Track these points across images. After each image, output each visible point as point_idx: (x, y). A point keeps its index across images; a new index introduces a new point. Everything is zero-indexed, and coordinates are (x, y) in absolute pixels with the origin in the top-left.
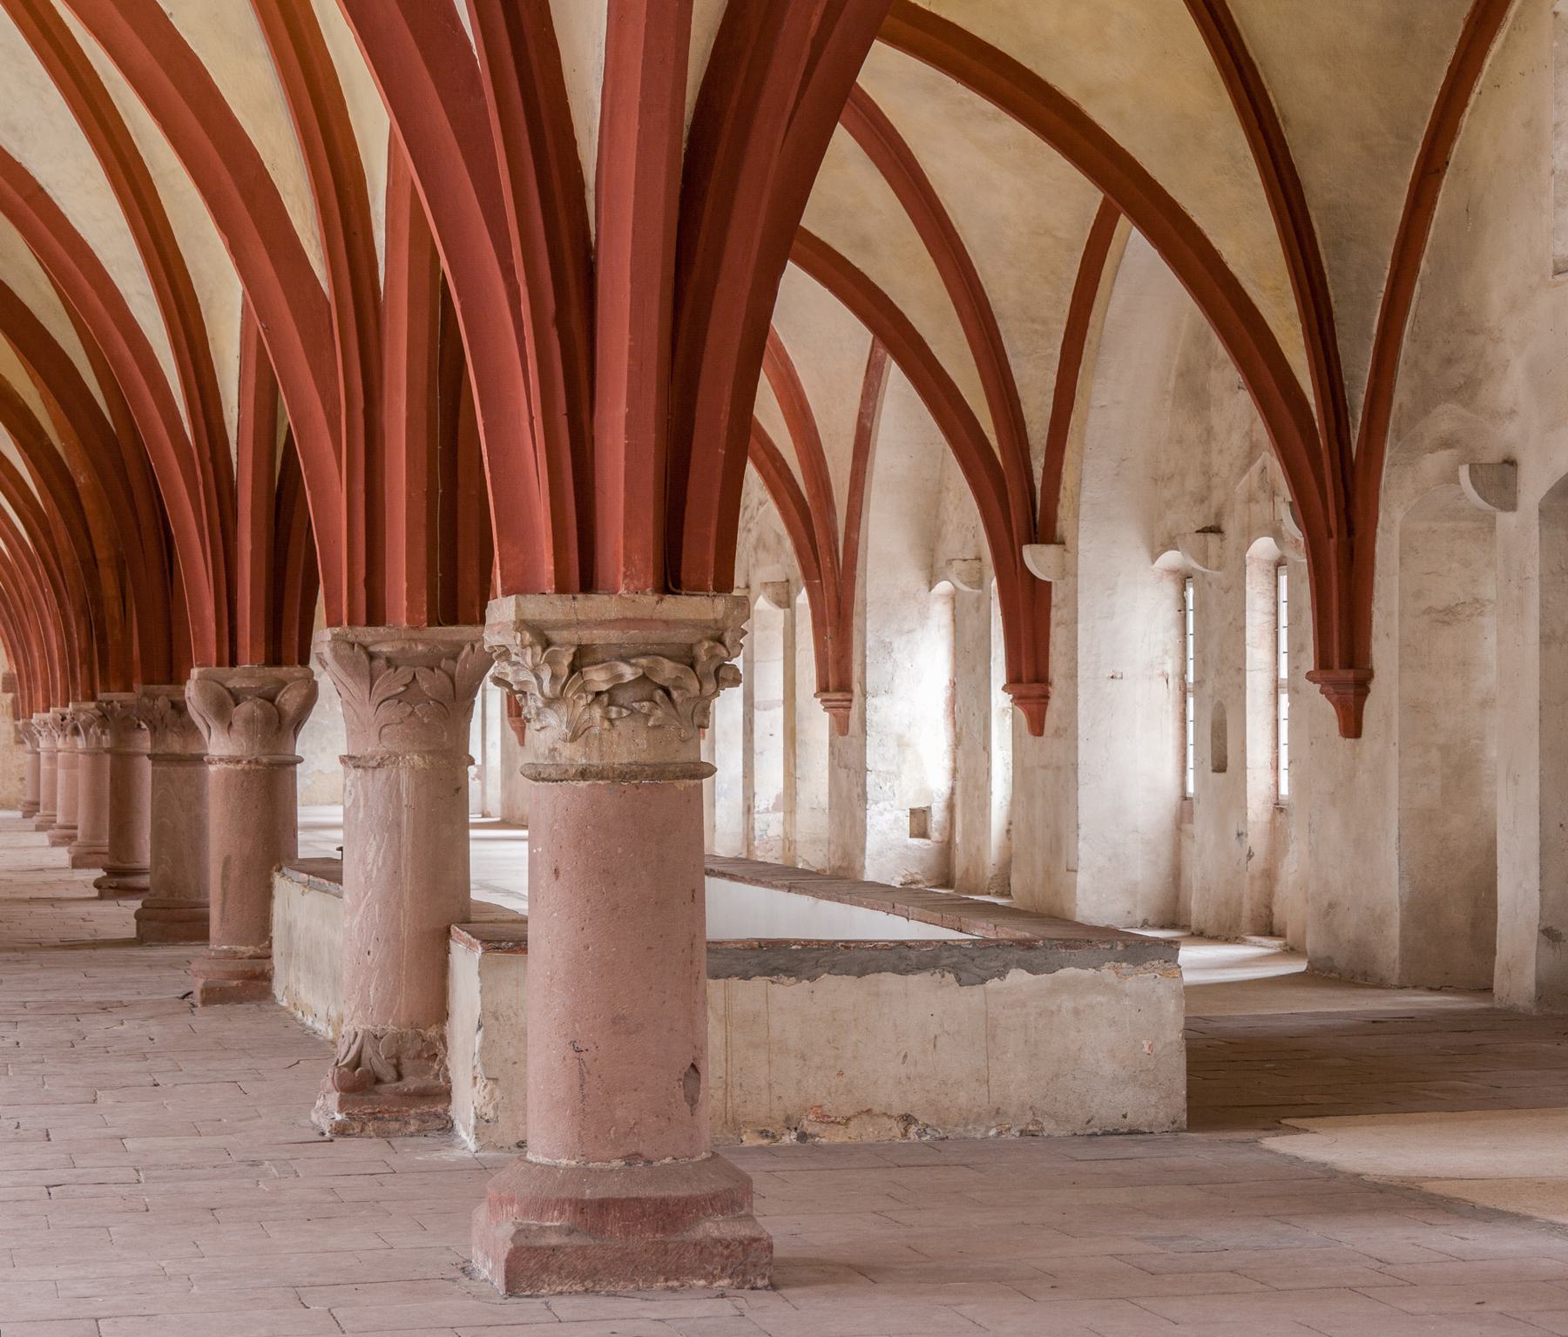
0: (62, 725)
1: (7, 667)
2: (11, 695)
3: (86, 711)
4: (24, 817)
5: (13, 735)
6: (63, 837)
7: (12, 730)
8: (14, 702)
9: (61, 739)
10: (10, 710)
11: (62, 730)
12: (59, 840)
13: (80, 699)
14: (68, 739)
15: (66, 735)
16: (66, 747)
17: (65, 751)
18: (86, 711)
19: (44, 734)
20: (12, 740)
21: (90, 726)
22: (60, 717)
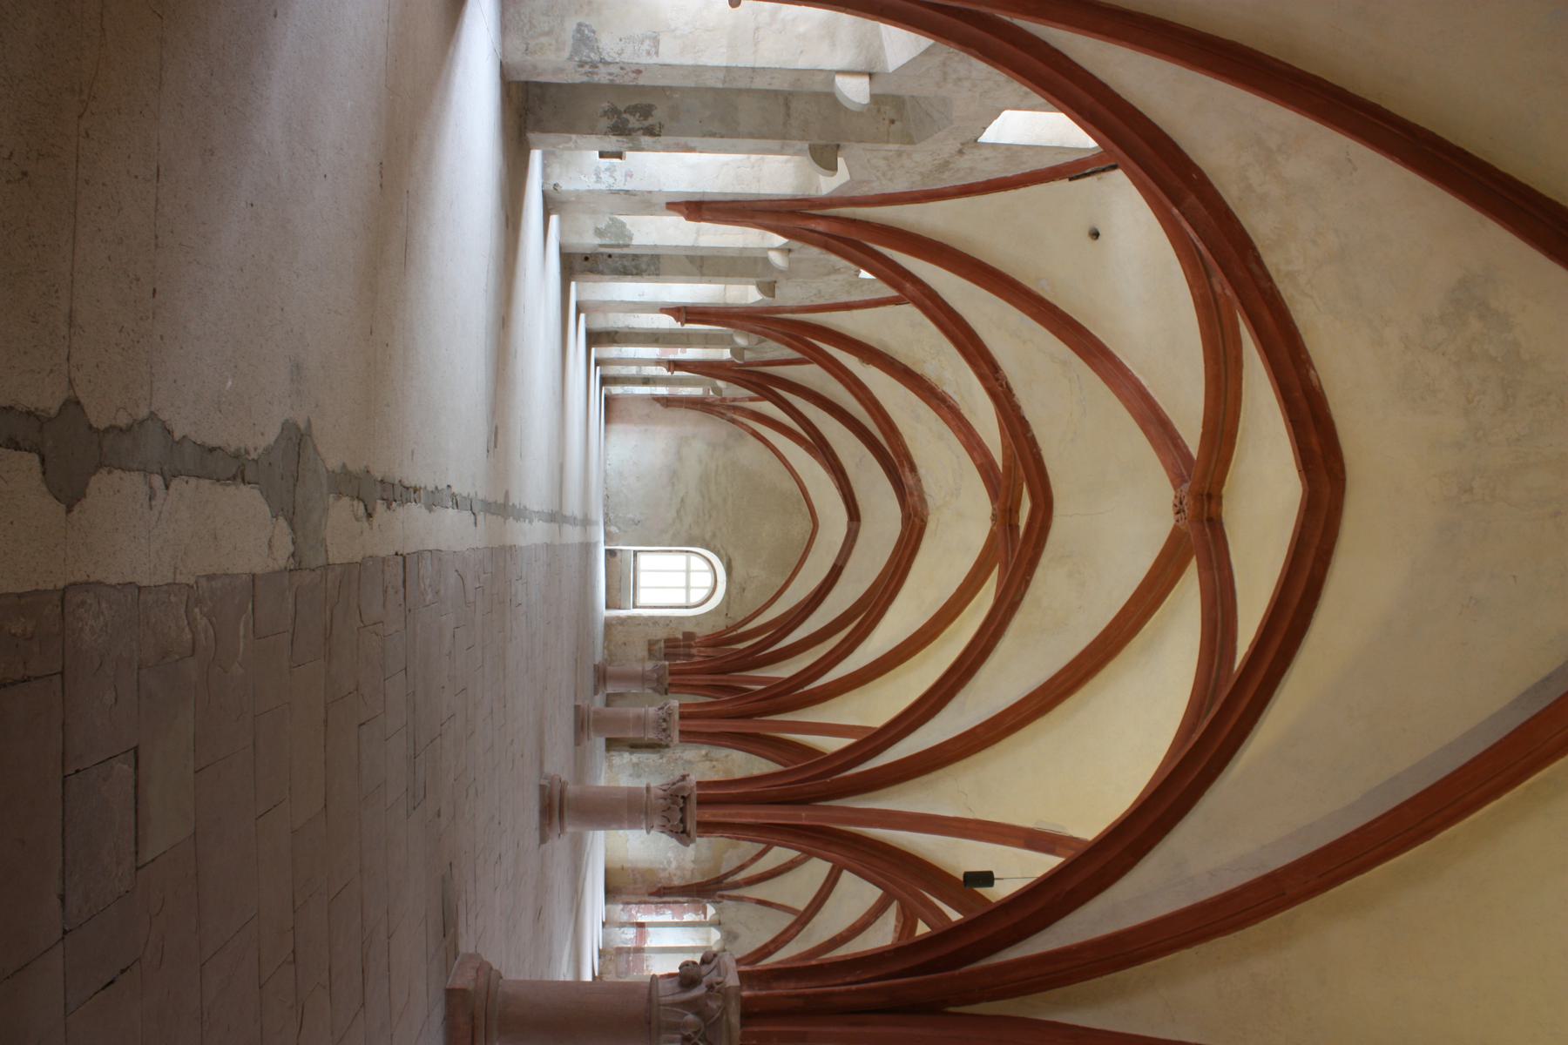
0: (677, 796)
1: (700, 635)
2: (681, 637)
3: (724, 1010)
4: (595, 665)
5: (655, 638)
6: (550, 797)
7: (658, 638)
8: (676, 640)
9: (662, 793)
10: (671, 637)
11: (671, 795)
12: (547, 793)
13: (746, 993)
14: (661, 801)
15: (665, 799)
16: (652, 796)
17: (647, 797)
18: (725, 1009)
19: (660, 712)
20: (649, 638)
21: (697, 1014)
22: (686, 795)
